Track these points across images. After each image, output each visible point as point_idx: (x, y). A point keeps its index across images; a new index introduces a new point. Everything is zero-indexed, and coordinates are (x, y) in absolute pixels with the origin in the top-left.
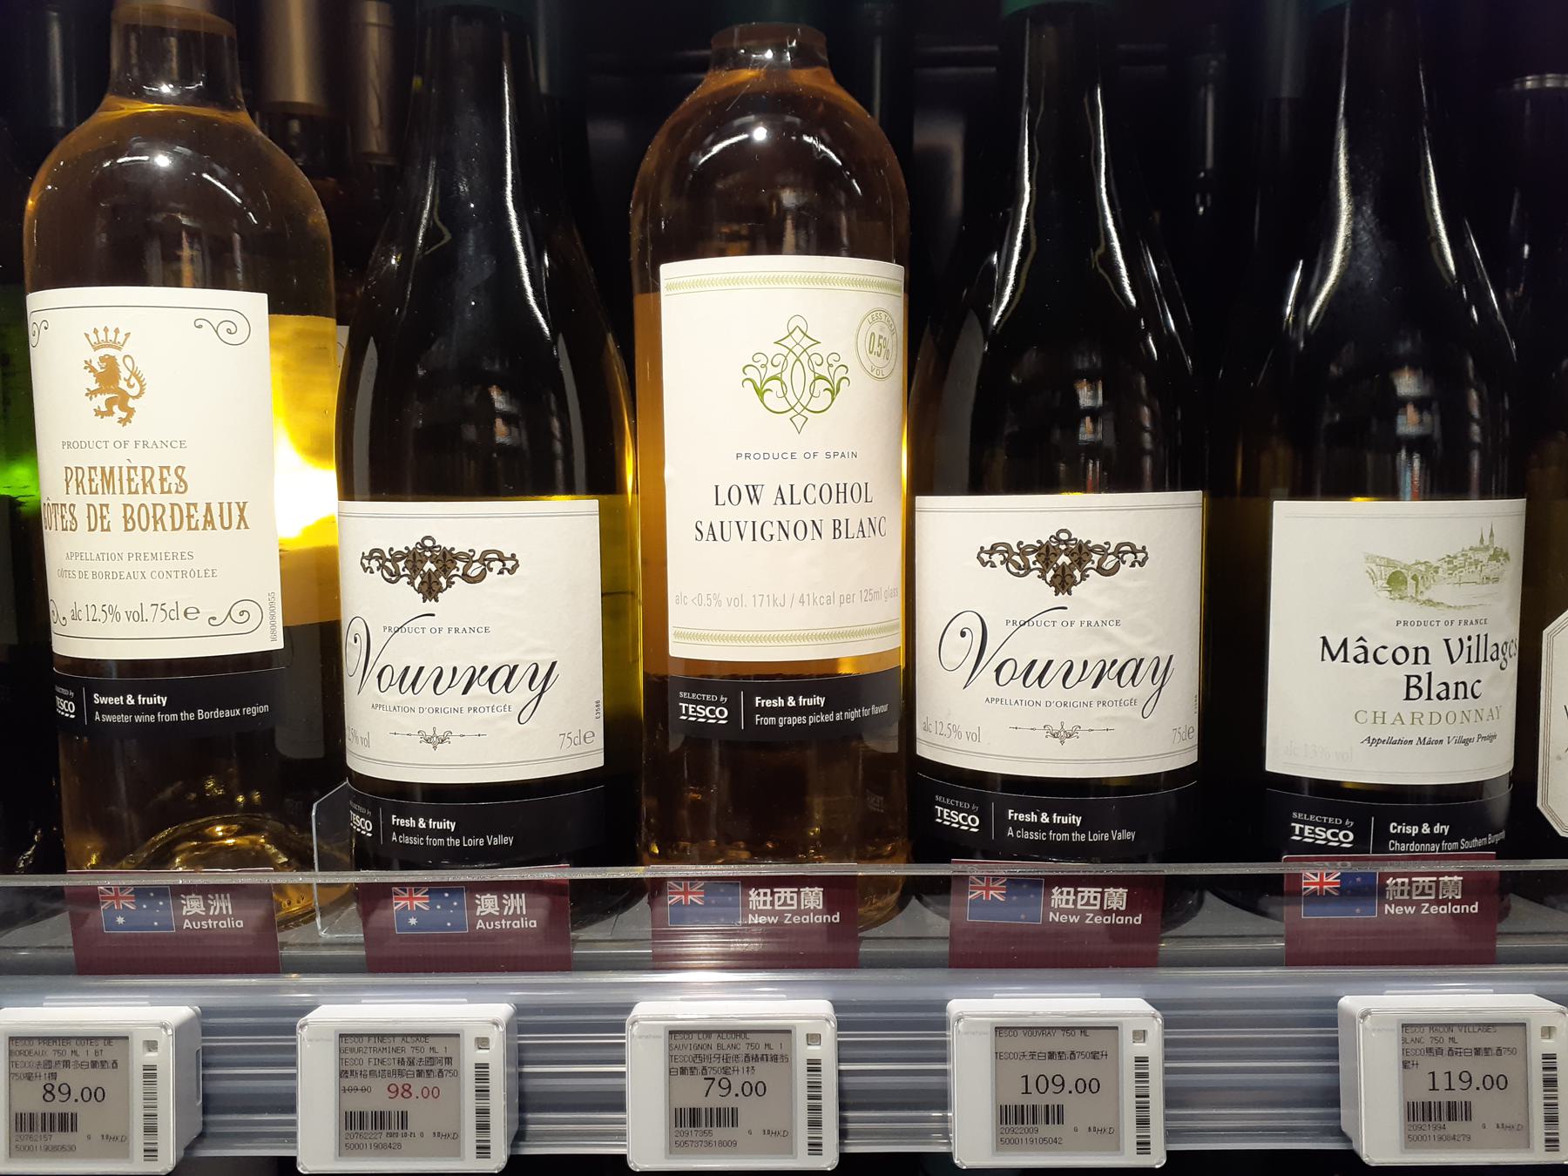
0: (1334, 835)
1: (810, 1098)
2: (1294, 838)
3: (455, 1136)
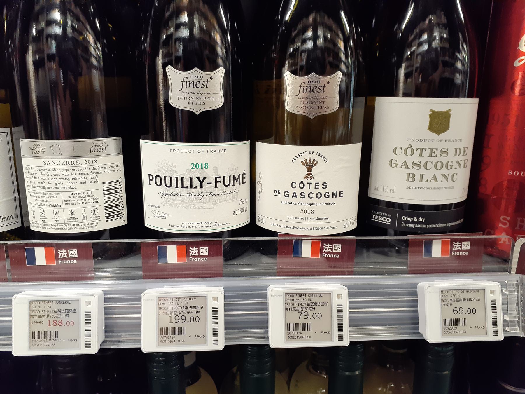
0: (384, 219)
1: (339, 319)
2: (372, 219)
3: (204, 337)
